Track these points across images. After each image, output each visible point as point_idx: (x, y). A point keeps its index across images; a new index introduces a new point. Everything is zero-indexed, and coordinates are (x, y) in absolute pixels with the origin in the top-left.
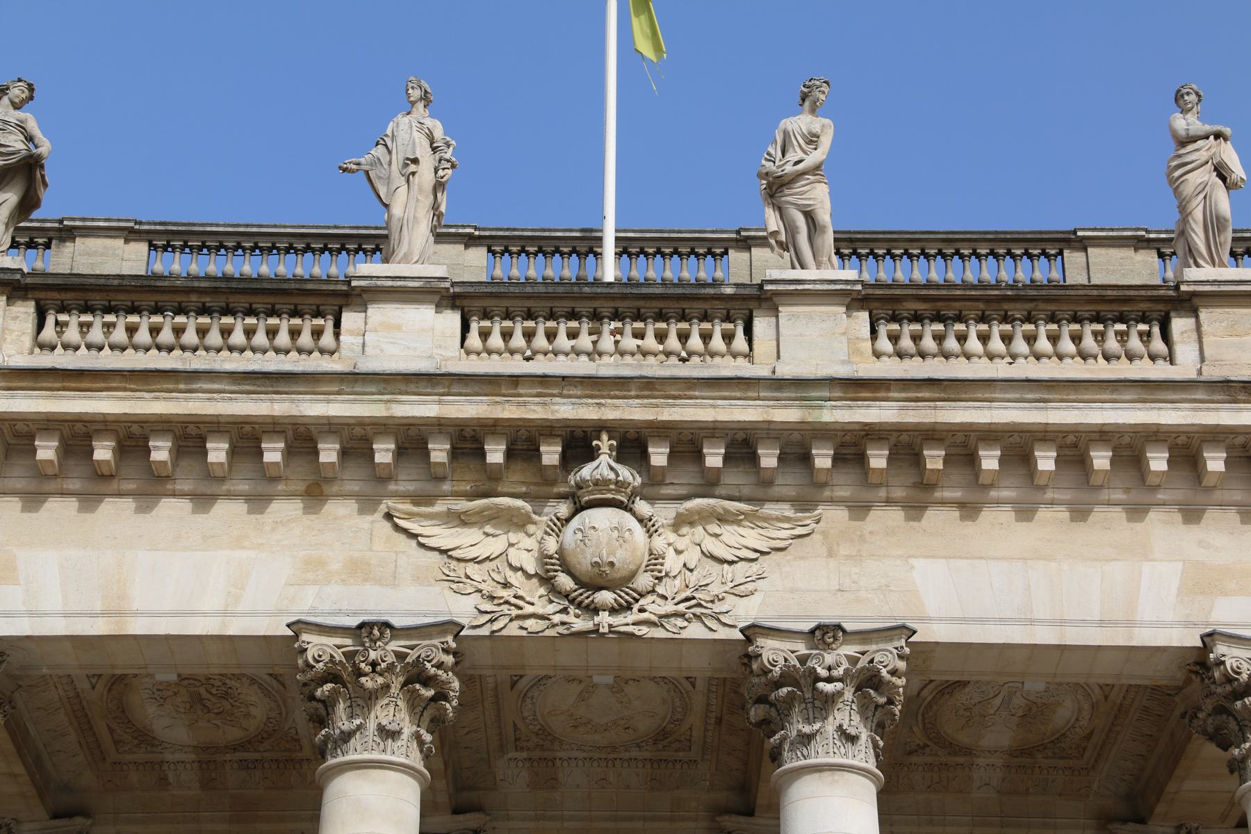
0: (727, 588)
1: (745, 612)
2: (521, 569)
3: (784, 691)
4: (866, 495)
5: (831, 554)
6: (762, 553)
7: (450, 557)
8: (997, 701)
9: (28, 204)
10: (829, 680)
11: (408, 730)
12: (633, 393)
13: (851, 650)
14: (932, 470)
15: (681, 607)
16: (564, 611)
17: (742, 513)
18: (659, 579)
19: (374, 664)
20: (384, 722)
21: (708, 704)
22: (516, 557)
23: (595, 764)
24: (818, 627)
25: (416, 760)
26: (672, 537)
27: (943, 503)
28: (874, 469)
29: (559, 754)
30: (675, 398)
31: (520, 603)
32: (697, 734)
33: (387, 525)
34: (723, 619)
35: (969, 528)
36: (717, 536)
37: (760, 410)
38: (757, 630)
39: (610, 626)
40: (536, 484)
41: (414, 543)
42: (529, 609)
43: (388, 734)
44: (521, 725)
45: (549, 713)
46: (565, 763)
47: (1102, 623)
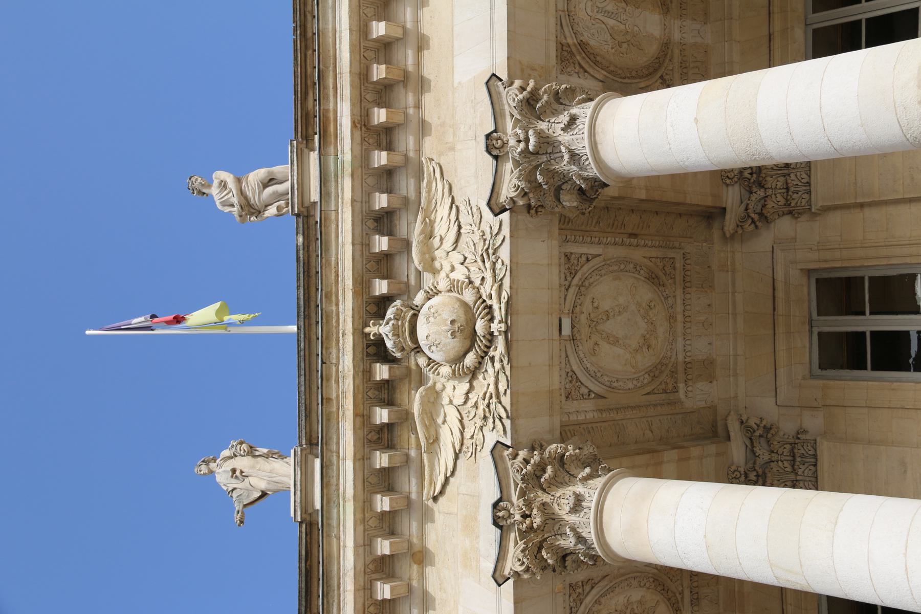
0: (476, 229)
2: (467, 394)
3: (540, 178)
4: (413, 125)
5: (452, 149)
6: (453, 202)
7: (460, 451)
8: (611, 22)
10: (527, 140)
11: (579, 489)
12: (334, 308)
13: (509, 124)
14: (387, 73)
15: (488, 265)
16: (492, 359)
17: (424, 220)
18: (471, 282)
19: (525, 516)
20: (568, 509)
21: (615, 244)
22: (459, 400)
23: (688, 331)
24: (488, 151)
25: (598, 482)
26: (443, 274)
27: (418, 64)
28: (387, 118)
29: (681, 358)
30: (337, 275)
31: (488, 395)
32: (654, 253)
33: (442, 500)
34: (495, 231)
35: (434, 43)
36: (441, 239)
37: (345, 209)
38: (493, 202)
39: (500, 322)
40: (410, 383)
41: (452, 480)
42: (492, 389)
43: (578, 504)
44: (648, 389)
45: (633, 367)
46: (688, 354)
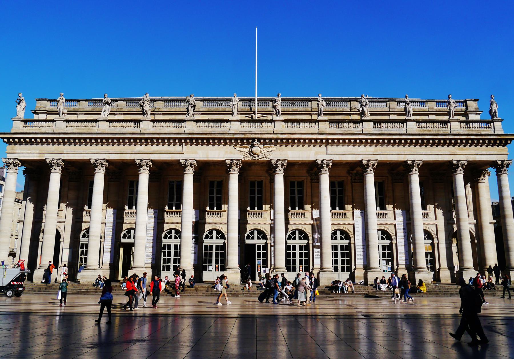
1: (270, 158)
9: (194, 109)
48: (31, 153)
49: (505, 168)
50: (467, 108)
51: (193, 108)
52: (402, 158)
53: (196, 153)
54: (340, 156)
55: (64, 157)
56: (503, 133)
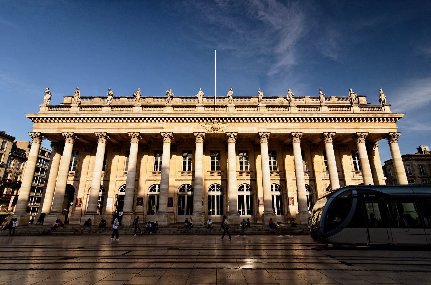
13: (233, 134)
47: (251, 131)
48: (51, 128)
49: (396, 138)
50: (359, 102)
51: (171, 98)
52: (320, 131)
53: (173, 128)
54: (275, 130)
55: (76, 131)
56: (391, 113)
